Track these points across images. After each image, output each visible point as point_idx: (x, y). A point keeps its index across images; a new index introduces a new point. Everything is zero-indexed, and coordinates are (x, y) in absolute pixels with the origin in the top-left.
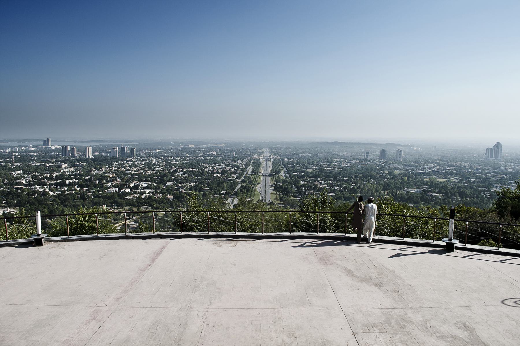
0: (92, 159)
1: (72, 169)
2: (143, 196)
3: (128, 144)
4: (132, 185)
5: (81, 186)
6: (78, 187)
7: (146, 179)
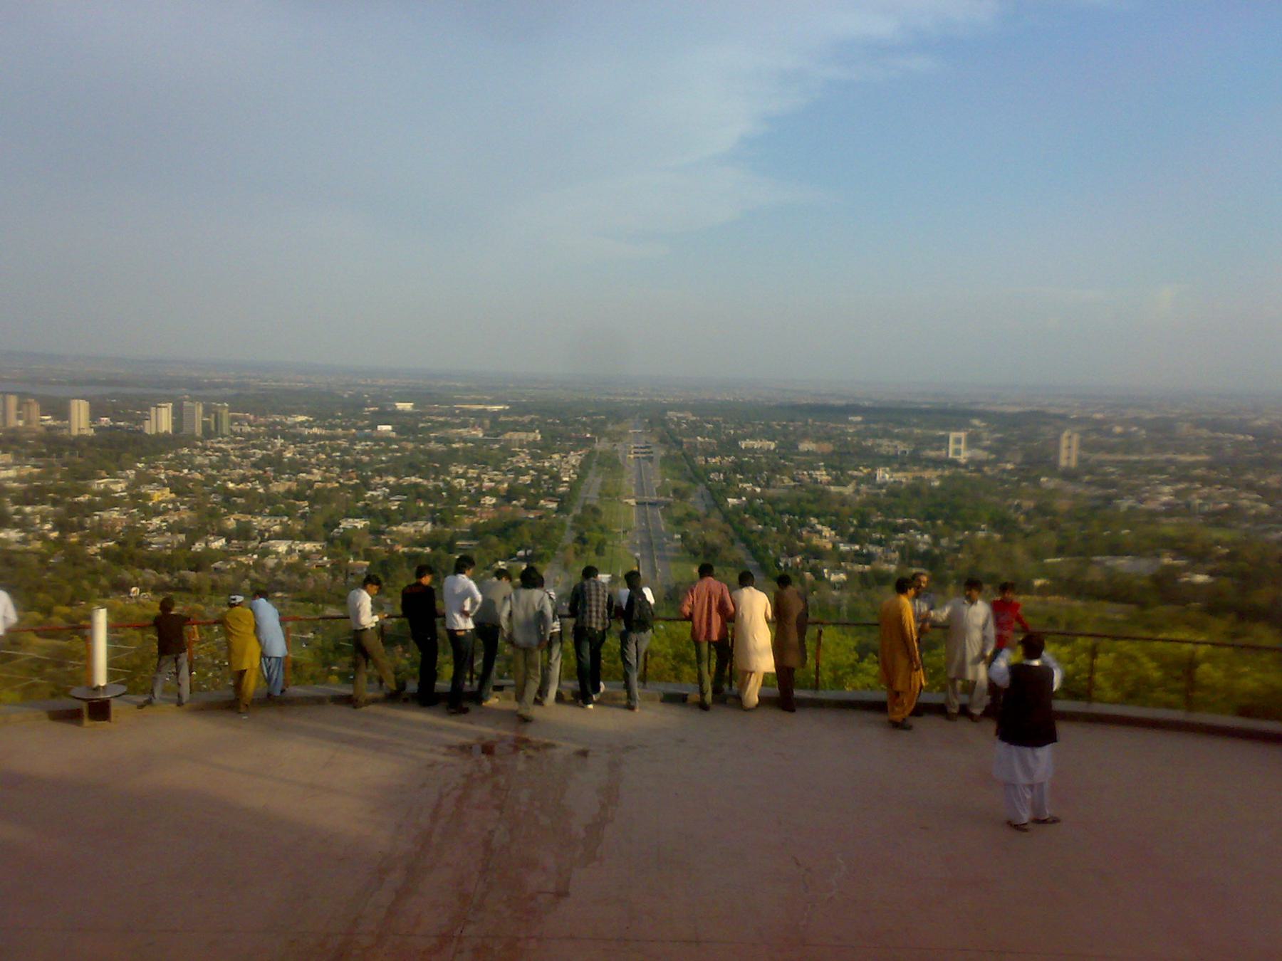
0: (91, 442)
1: (28, 469)
2: (271, 562)
3: (201, 393)
4: (231, 523)
5: (59, 526)
6: (53, 530)
7: (269, 503)
